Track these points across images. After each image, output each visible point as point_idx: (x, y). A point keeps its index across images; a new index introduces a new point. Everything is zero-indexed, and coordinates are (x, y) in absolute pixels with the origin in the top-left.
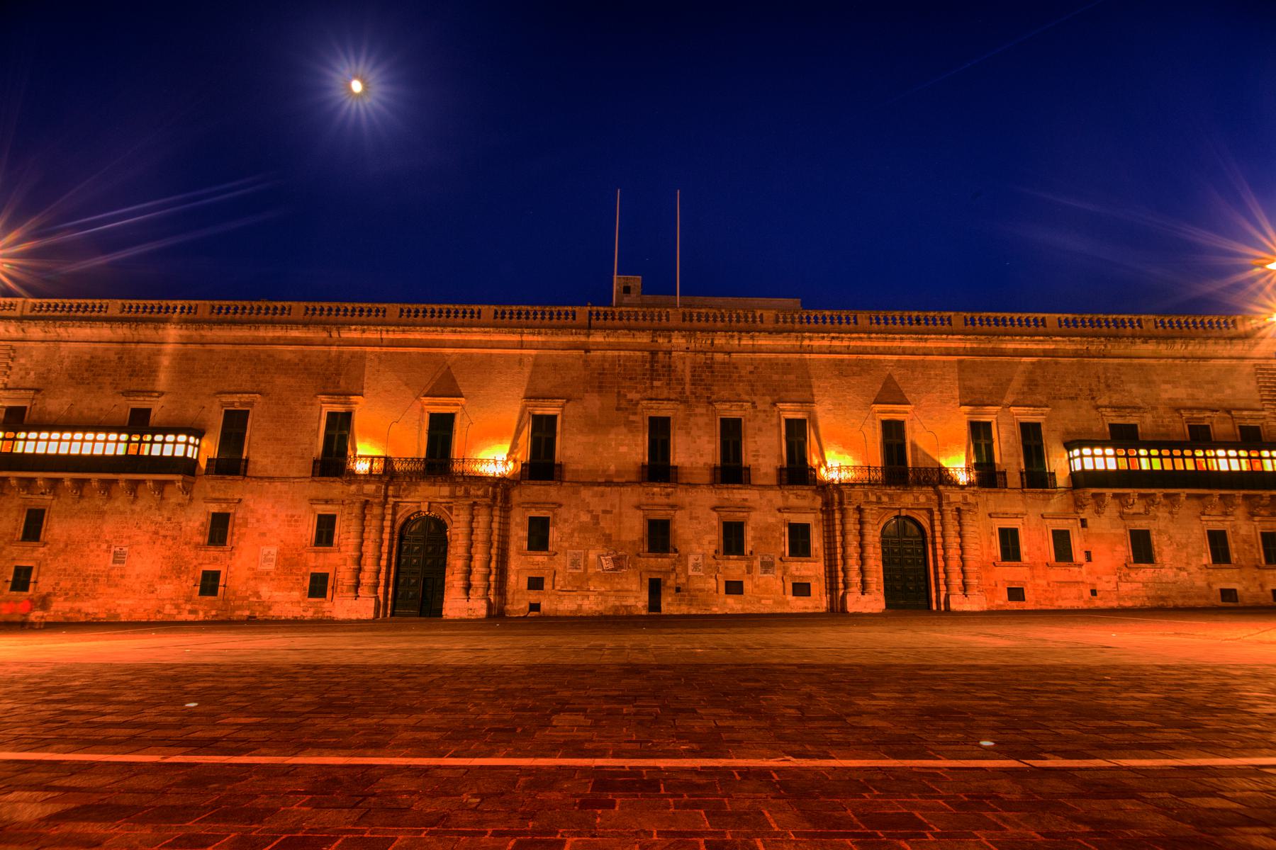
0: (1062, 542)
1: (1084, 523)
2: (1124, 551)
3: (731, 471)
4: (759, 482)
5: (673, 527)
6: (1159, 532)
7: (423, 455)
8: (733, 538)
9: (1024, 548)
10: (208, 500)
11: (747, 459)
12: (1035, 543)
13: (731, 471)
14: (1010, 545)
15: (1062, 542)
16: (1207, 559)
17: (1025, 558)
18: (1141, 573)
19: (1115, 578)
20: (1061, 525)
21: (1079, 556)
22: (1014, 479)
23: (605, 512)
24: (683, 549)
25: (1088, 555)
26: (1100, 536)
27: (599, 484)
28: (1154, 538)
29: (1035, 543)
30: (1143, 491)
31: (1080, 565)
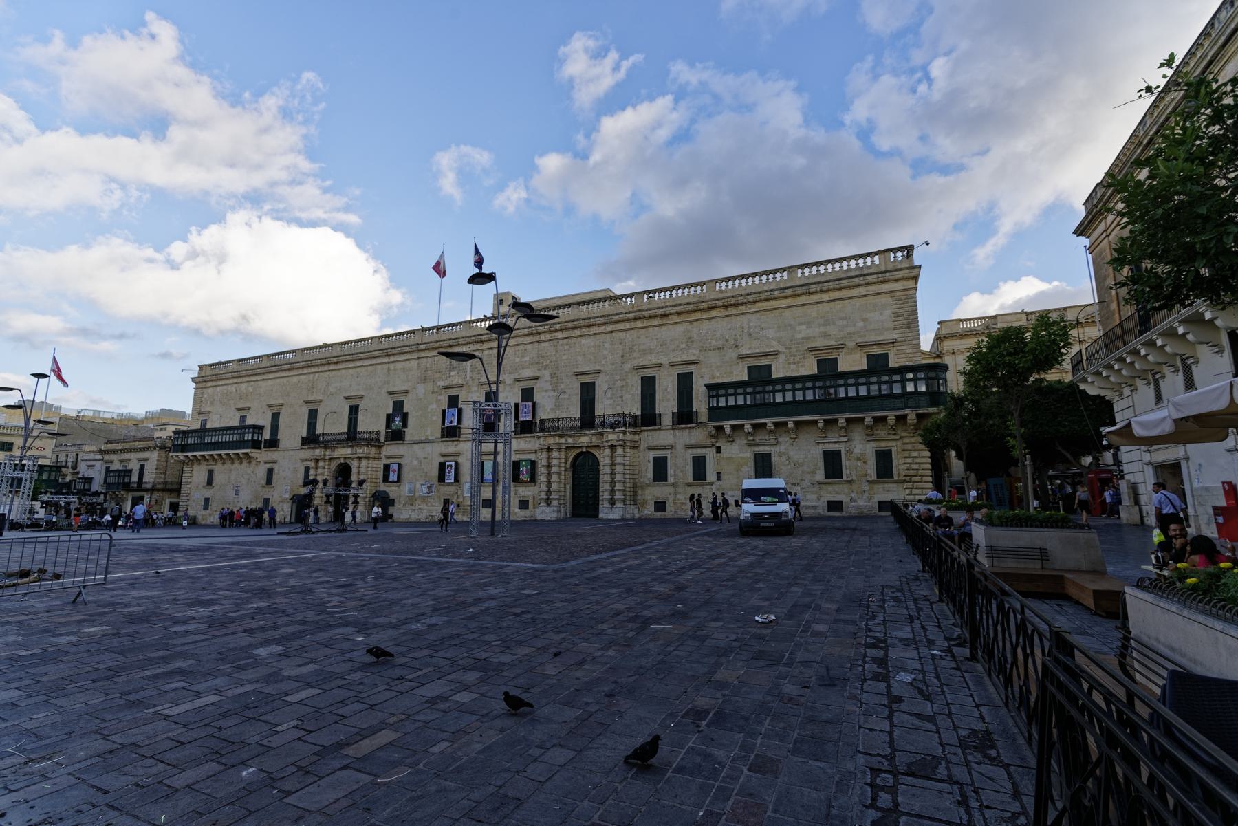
0: (699, 466)
1: (718, 450)
4: (416, 438)
6: (780, 454)
7: (346, 430)
9: (670, 472)
12: (680, 468)
14: (660, 467)
15: (699, 466)
17: (671, 480)
21: (711, 476)
22: (667, 420)
25: (719, 474)
26: (730, 459)
28: (775, 459)
29: (680, 468)
31: (711, 484)
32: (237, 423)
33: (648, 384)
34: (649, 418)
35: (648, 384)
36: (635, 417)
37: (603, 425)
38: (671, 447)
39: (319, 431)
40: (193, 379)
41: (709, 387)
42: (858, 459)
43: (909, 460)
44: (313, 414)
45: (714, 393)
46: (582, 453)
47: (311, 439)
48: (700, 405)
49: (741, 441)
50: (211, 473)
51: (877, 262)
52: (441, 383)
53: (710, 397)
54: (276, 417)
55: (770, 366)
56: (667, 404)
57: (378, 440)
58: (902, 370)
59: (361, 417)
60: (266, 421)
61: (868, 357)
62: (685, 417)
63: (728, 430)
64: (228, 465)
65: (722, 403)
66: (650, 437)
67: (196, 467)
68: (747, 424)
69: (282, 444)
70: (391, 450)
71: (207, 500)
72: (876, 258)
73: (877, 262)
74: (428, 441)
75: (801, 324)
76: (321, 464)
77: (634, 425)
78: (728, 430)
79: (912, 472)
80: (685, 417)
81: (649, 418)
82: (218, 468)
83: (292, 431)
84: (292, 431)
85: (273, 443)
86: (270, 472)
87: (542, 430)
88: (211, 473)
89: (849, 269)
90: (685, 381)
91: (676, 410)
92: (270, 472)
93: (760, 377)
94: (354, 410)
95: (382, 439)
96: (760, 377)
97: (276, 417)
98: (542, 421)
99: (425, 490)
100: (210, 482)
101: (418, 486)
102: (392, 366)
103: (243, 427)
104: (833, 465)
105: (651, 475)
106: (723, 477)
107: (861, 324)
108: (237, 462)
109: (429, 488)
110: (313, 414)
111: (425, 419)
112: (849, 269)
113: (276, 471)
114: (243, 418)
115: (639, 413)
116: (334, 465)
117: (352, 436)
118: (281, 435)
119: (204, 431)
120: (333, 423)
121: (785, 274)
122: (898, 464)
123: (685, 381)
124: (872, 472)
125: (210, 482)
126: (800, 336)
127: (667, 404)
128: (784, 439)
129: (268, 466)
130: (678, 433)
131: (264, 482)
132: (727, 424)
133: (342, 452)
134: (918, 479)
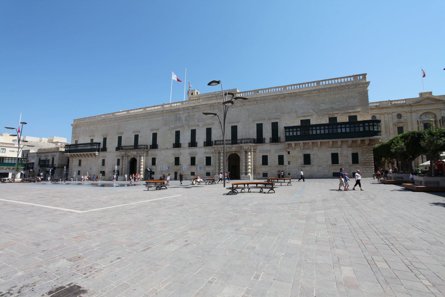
0: (281, 160)
1: (289, 153)
2: (301, 160)
3: (193, 144)
5: (180, 159)
6: (314, 155)
7: (133, 145)
8: (193, 161)
9: (269, 161)
10: (102, 157)
11: (197, 140)
12: (273, 160)
13: (193, 144)
14: (265, 160)
15: (281, 160)
16: (330, 162)
17: (269, 164)
18: (306, 168)
19: (297, 169)
20: (281, 154)
21: (286, 163)
23: (166, 156)
24: (182, 164)
25: (289, 163)
27: (165, 149)
28: (312, 157)
29: (273, 160)
30: (305, 142)
31: (286, 166)
32: (89, 141)
33: (260, 127)
34: (260, 140)
35: (260, 127)
36: (254, 140)
37: (241, 143)
38: (269, 151)
39: (123, 144)
40: (72, 125)
41: (286, 128)
42: (345, 156)
43: (365, 157)
44: (120, 139)
45: (287, 130)
46: (232, 154)
47: (119, 148)
48: (281, 134)
49: (298, 149)
50: (80, 161)
51: (352, 80)
52: (172, 126)
53: (286, 132)
54: (105, 140)
55: (310, 120)
56: (267, 134)
57: (147, 148)
58: (364, 122)
59: (139, 139)
60: (101, 141)
61: (349, 117)
62: (275, 139)
63: (293, 145)
64: (87, 158)
65: (291, 134)
66: (260, 147)
67: (74, 159)
68: (301, 142)
69: (108, 150)
70: (153, 153)
71: (79, 172)
72: (352, 78)
73: (352, 80)
74: (167, 148)
75: (322, 103)
76: (124, 158)
77: (254, 143)
78: (293, 145)
79: (365, 162)
80: (275, 139)
81: (260, 140)
82: (83, 159)
83: (112, 144)
84: (112, 144)
85: (104, 149)
86: (104, 161)
87: (215, 144)
88: (80, 161)
89: (341, 82)
90: (275, 126)
91: (271, 137)
92: (104, 161)
93: (305, 124)
94: (136, 137)
95: (149, 147)
96: (305, 124)
97: (105, 140)
98: (215, 141)
99: (167, 168)
100: (80, 164)
101: (164, 167)
102: (152, 119)
103: (92, 144)
104: (335, 158)
105: (261, 163)
106: (291, 163)
107: (346, 104)
108: (90, 157)
109: (169, 167)
110: (120, 139)
111: (166, 140)
112: (341, 82)
113: (106, 161)
114: (92, 140)
115: (256, 138)
116: (129, 159)
117: (136, 146)
118: (107, 147)
119: (76, 145)
120: (128, 141)
121: (315, 84)
122: (360, 158)
123: (275, 126)
124: (351, 161)
125: (80, 164)
126: (322, 108)
127: (267, 134)
128: (316, 149)
129: (103, 158)
130: (272, 146)
131: (101, 164)
132: (293, 143)
133: (133, 153)
134: (368, 164)
